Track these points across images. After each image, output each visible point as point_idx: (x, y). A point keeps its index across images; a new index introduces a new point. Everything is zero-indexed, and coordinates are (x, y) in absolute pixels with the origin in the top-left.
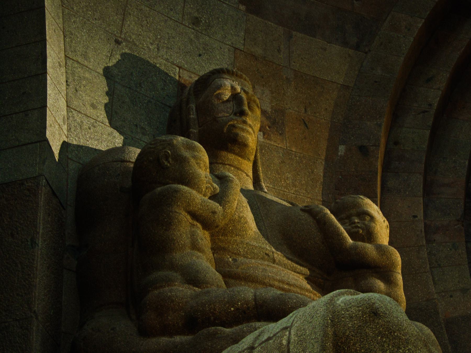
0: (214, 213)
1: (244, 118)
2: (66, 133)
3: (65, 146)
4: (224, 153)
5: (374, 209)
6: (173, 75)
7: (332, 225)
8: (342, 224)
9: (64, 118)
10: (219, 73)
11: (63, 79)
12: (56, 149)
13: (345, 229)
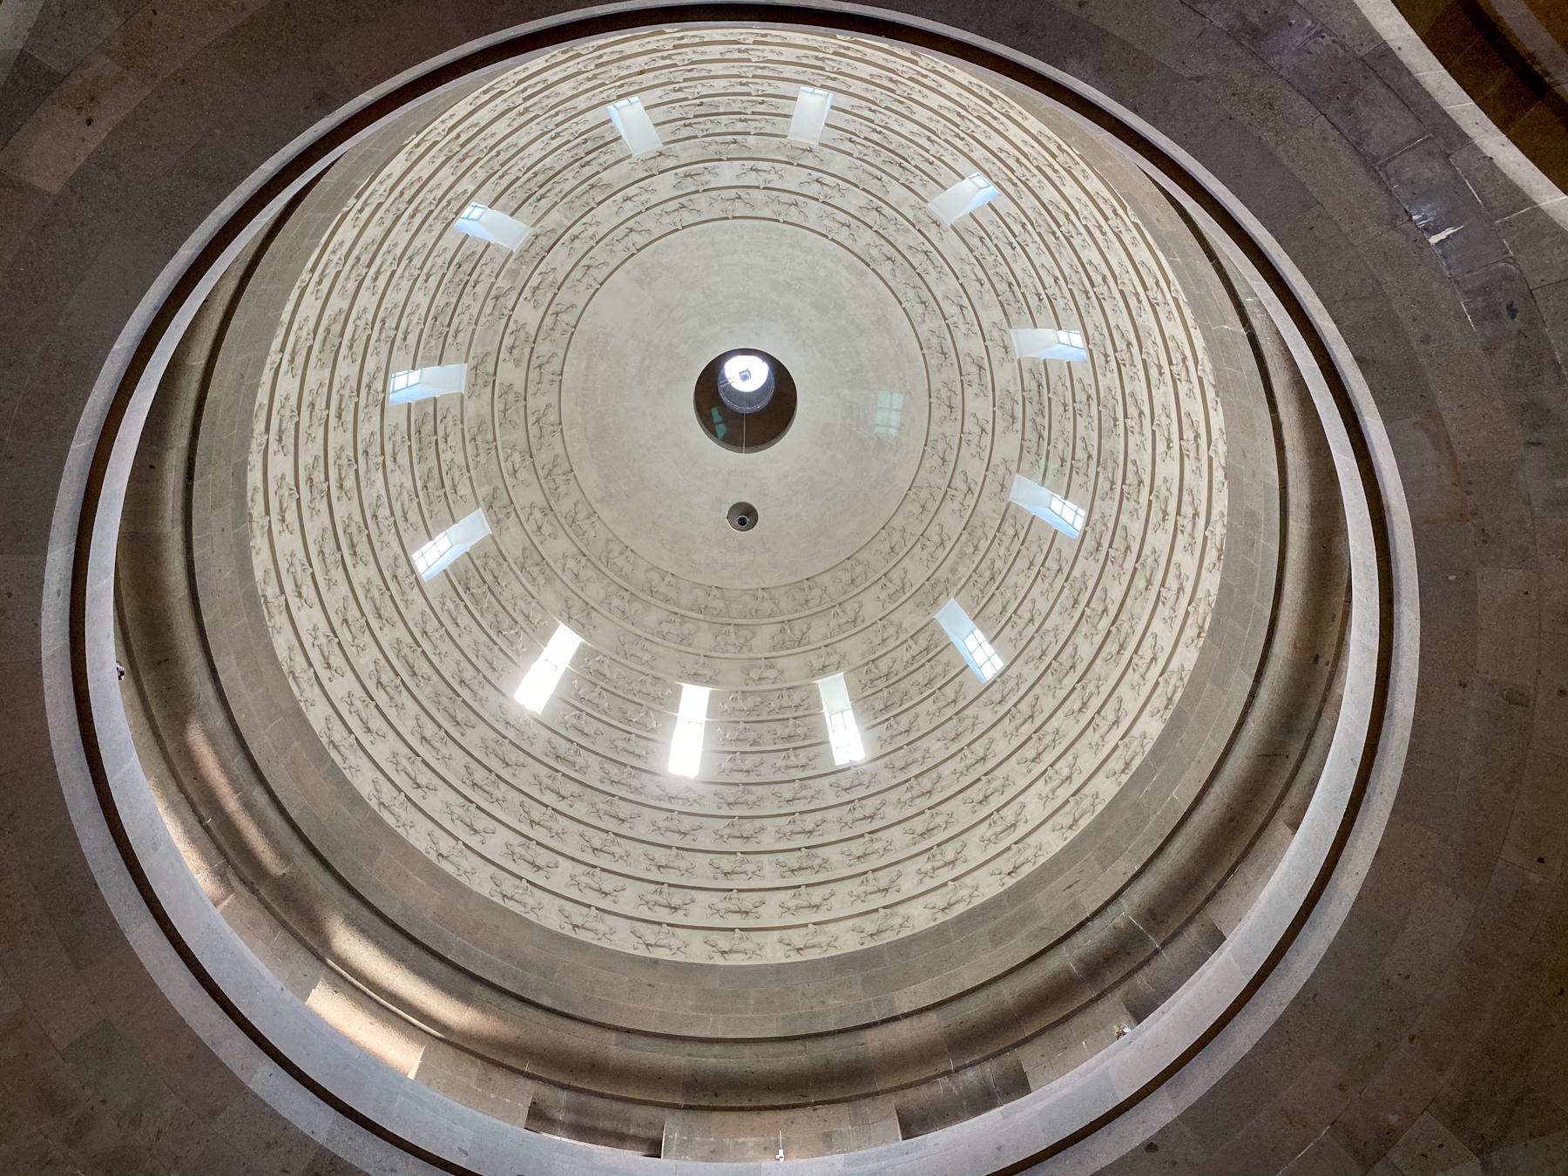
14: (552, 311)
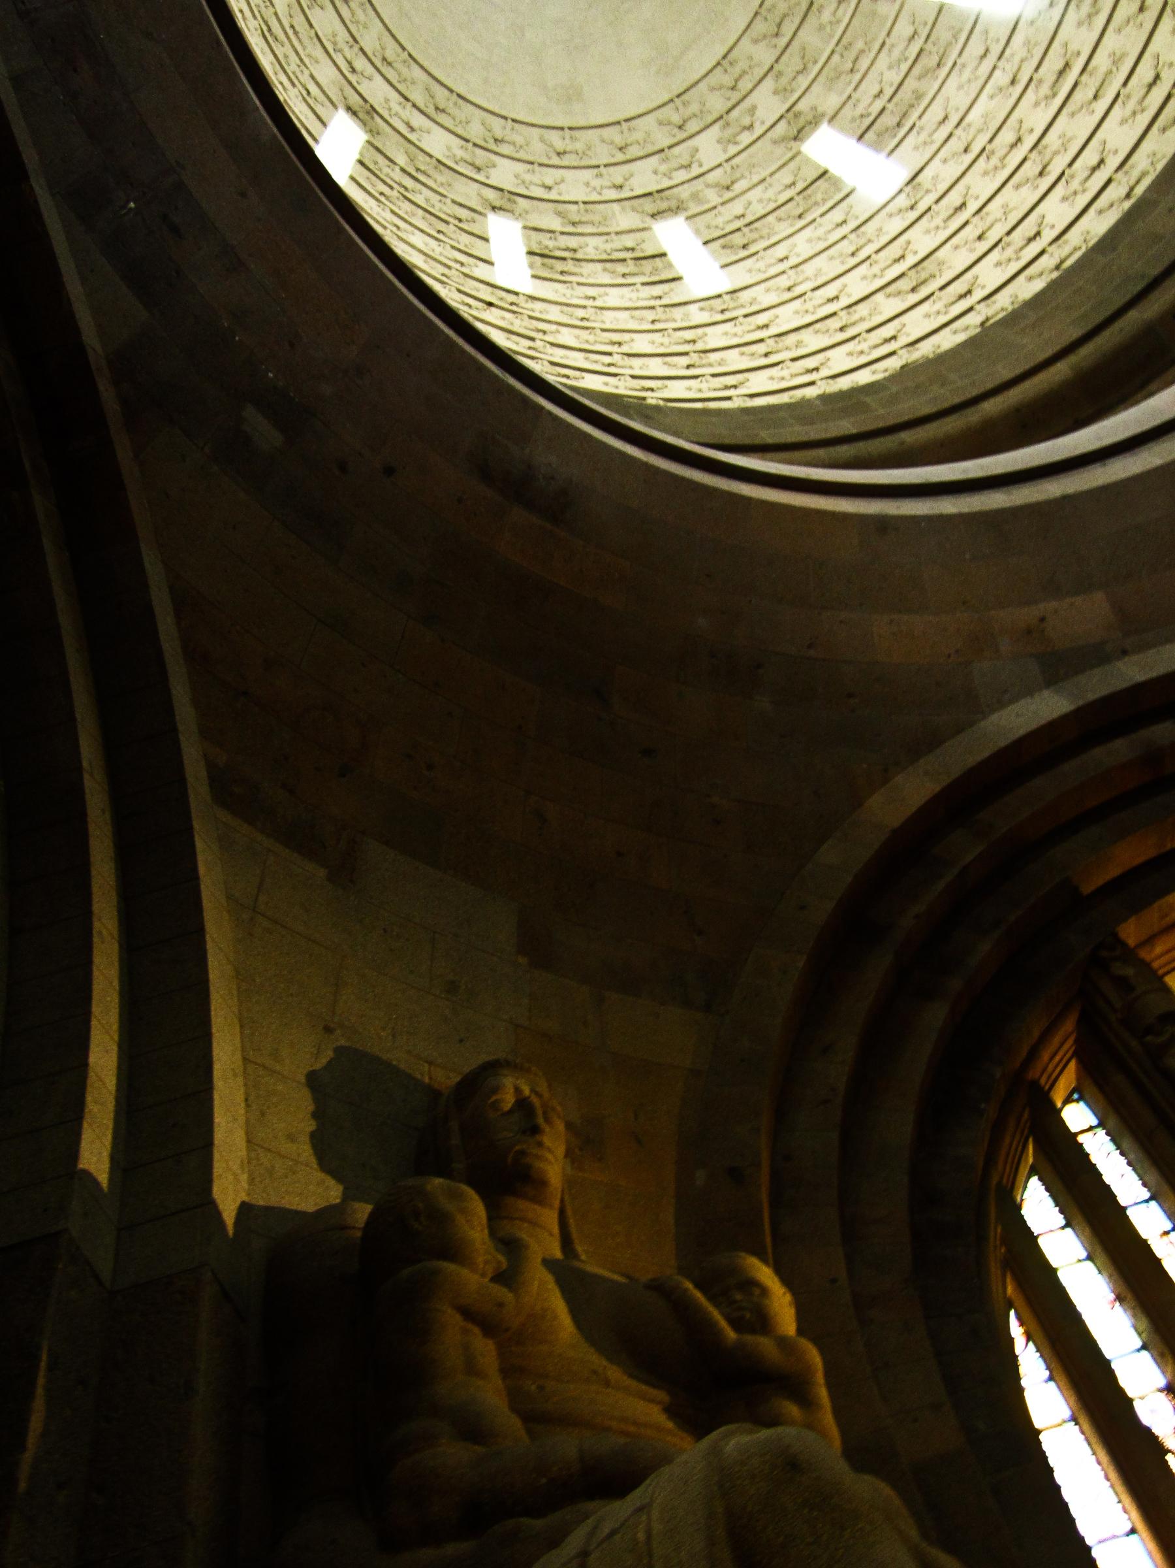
0: (501, 1305)
1: (538, 1137)
2: (246, 1185)
3: (245, 1209)
5: (765, 1274)
6: (419, 1077)
8: (716, 1306)
9: (242, 1162)
10: (492, 1067)
11: (240, 1096)
12: (229, 1215)
13: (722, 1314)
14: (684, 132)
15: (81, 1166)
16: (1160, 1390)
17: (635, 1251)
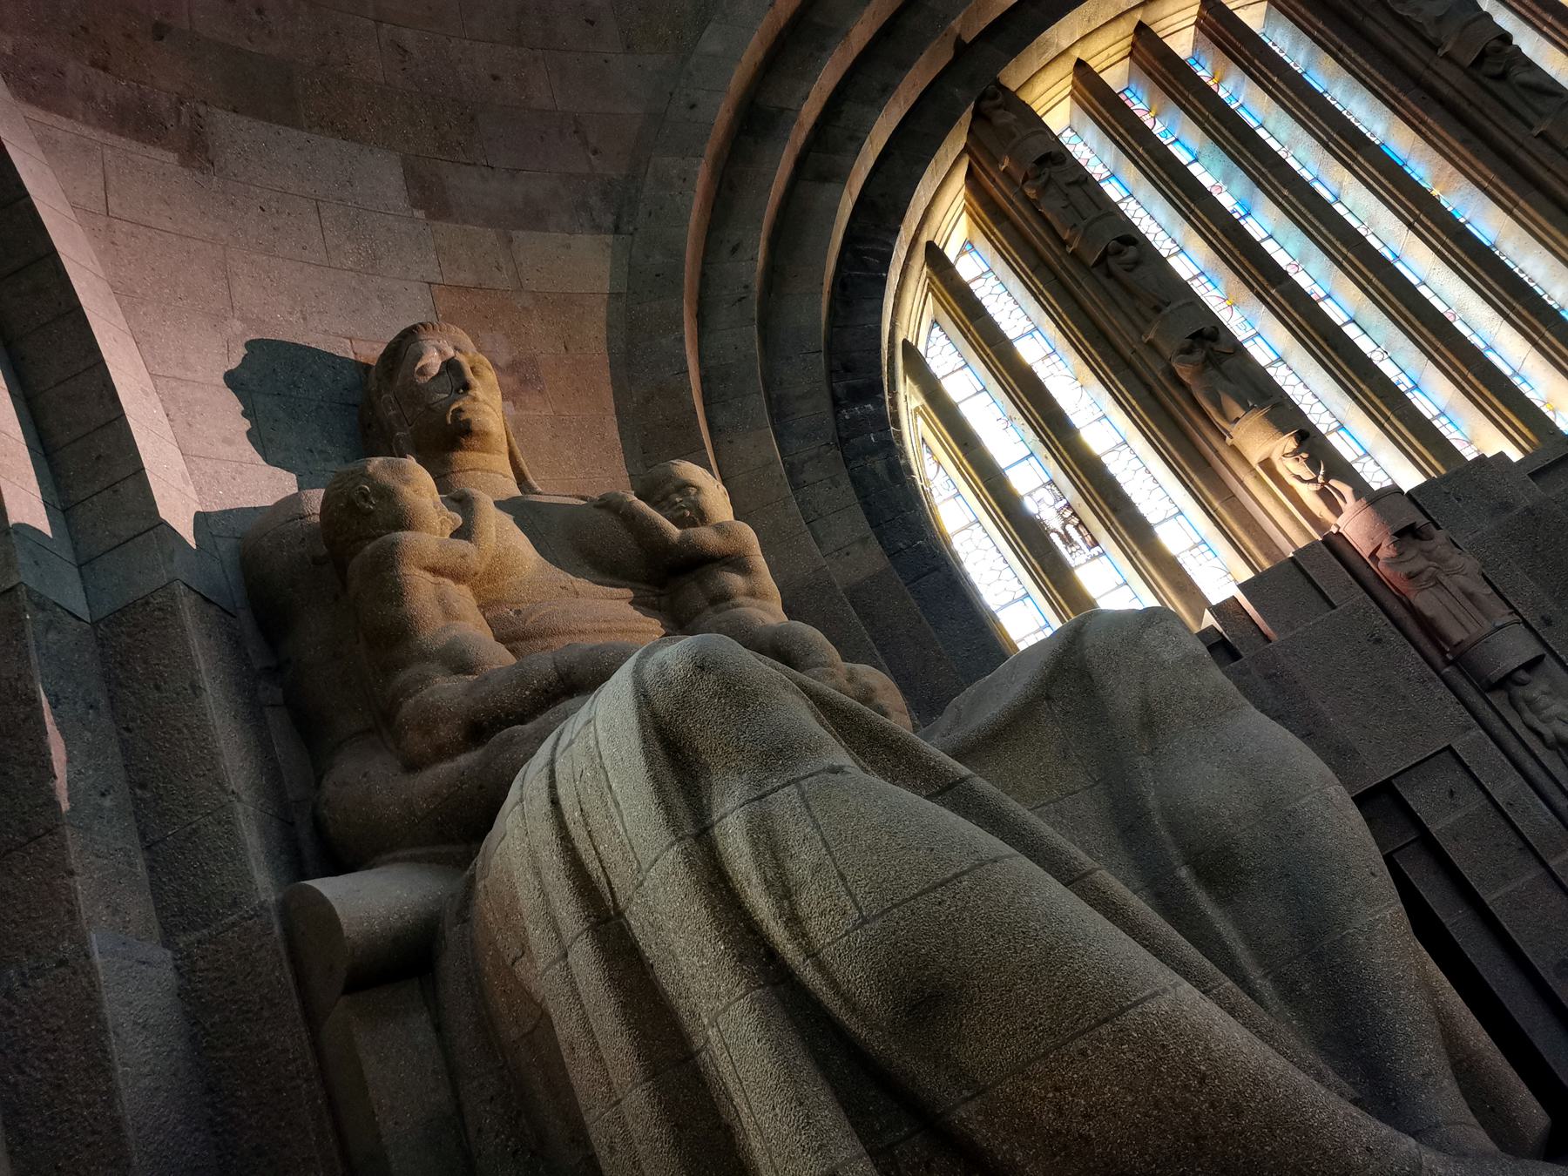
2: (195, 497)
3: (201, 520)
4: (458, 455)
7: (644, 517)
8: (660, 510)
9: (183, 475)
15: (12, 520)
16: (1044, 485)
17: (588, 471)
